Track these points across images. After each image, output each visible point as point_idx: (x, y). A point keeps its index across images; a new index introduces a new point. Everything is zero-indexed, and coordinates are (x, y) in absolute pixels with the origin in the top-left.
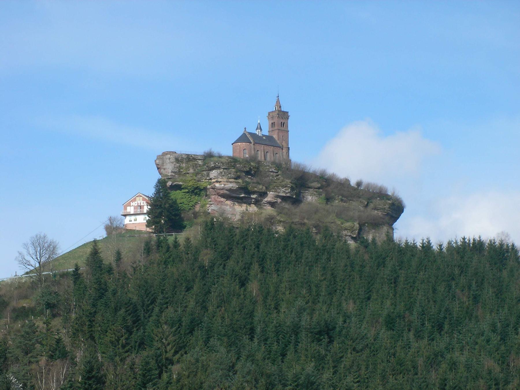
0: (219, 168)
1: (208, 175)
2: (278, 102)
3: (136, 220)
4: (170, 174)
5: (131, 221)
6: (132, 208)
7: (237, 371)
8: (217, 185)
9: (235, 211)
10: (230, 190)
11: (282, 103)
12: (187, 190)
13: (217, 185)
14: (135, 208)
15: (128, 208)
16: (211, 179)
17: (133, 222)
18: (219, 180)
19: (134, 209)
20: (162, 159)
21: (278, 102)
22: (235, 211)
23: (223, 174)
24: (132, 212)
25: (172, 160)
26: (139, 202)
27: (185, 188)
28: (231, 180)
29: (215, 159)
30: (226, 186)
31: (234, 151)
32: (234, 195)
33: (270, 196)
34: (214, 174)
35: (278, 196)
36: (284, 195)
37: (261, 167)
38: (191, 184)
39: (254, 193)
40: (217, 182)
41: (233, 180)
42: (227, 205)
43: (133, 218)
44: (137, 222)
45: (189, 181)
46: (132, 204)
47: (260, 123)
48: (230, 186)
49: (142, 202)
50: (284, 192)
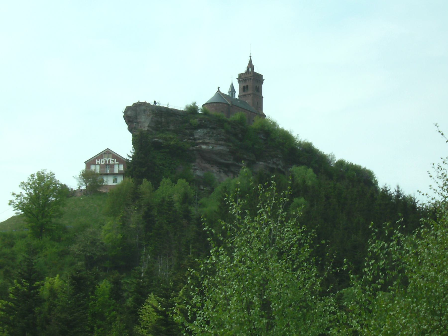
1: (192, 135)
2: (250, 62)
6: (98, 167)
8: (204, 147)
10: (219, 154)
13: (204, 147)
16: (195, 139)
18: (206, 141)
21: (250, 62)
26: (107, 160)
28: (220, 142)
34: (199, 133)
38: (172, 143)
40: (203, 143)
41: (222, 143)
48: (221, 148)
50: (274, 163)
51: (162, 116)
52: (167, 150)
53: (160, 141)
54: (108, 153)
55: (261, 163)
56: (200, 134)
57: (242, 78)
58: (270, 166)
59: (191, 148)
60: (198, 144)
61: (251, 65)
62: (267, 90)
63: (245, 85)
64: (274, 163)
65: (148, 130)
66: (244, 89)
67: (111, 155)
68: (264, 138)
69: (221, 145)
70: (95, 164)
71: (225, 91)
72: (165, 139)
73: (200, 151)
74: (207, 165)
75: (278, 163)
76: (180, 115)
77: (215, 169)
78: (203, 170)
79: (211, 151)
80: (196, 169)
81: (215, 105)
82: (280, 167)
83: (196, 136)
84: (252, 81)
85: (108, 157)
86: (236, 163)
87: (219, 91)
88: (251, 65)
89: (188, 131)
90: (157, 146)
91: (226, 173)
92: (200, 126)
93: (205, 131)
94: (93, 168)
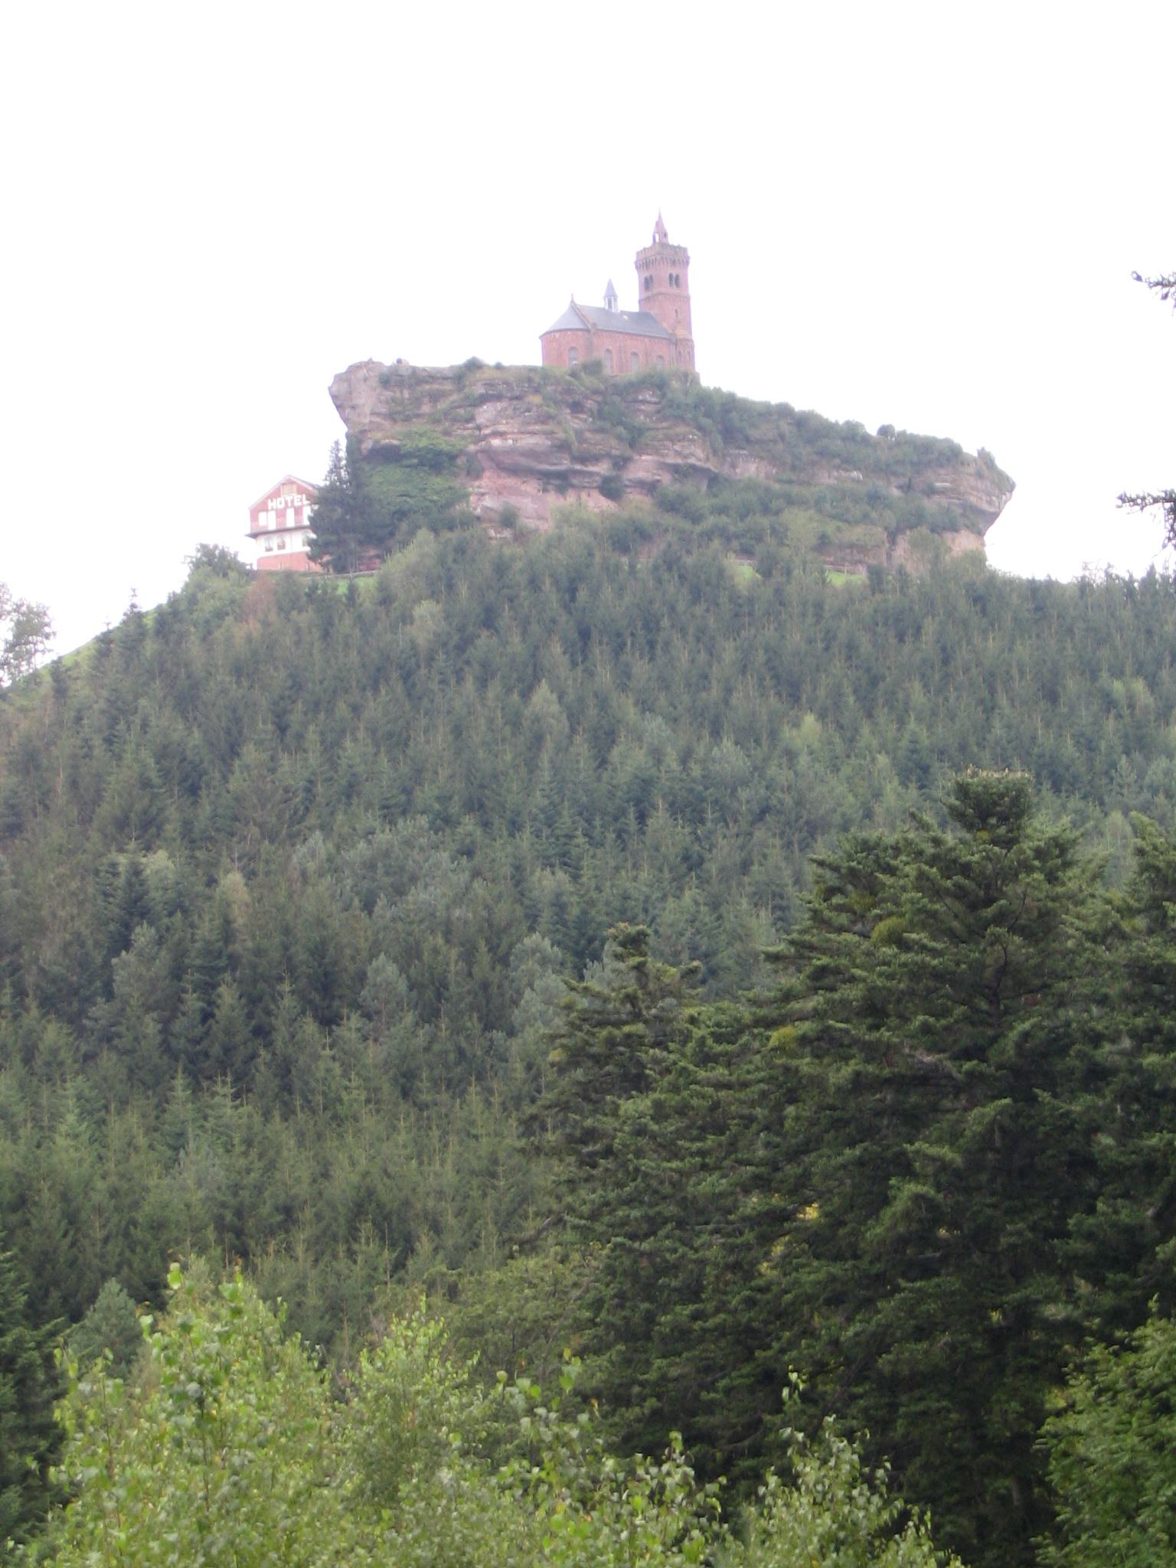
0: (499, 398)
1: (471, 419)
2: (659, 224)
3: (282, 546)
4: (367, 420)
5: (269, 550)
6: (272, 515)
8: (496, 442)
9: (539, 509)
10: (531, 453)
11: (668, 227)
12: (415, 461)
13: (496, 442)
14: (281, 514)
15: (262, 516)
16: (479, 428)
17: (276, 552)
18: (502, 428)
19: (278, 516)
20: (348, 381)
21: (659, 224)
22: (539, 509)
23: (510, 412)
24: (272, 527)
25: (374, 382)
26: (289, 499)
27: (410, 455)
29: (487, 375)
31: (546, 355)
32: (545, 467)
33: (643, 468)
34: (485, 413)
35: (664, 466)
36: (680, 461)
37: (619, 394)
38: (423, 443)
39: (596, 459)
40: (496, 434)
41: (537, 427)
42: (525, 494)
43: (275, 541)
44: (287, 551)
45: (422, 435)
46: (270, 504)
48: (528, 442)
49: (297, 497)
50: (678, 454)
51: (404, 387)
52: (415, 461)
53: (395, 442)
54: (289, 482)
55: (644, 457)
56: (487, 416)
57: (645, 262)
58: (670, 461)
59: (472, 448)
60: (485, 437)
61: (660, 230)
63: (647, 274)
64: (678, 454)
65: (371, 422)
67: (295, 487)
68: (654, 400)
70: (267, 511)
71: (594, 300)
72: (408, 435)
73: (489, 453)
74: (511, 481)
75: (686, 452)
76: (445, 378)
77: (531, 487)
78: (500, 493)
79: (511, 451)
80: (483, 494)
81: (557, 335)
82: (692, 461)
84: (663, 267)
86: (578, 467)
88: (660, 230)
89: (461, 411)
90: (388, 455)
91: (561, 490)
92: (483, 399)
93: (499, 406)
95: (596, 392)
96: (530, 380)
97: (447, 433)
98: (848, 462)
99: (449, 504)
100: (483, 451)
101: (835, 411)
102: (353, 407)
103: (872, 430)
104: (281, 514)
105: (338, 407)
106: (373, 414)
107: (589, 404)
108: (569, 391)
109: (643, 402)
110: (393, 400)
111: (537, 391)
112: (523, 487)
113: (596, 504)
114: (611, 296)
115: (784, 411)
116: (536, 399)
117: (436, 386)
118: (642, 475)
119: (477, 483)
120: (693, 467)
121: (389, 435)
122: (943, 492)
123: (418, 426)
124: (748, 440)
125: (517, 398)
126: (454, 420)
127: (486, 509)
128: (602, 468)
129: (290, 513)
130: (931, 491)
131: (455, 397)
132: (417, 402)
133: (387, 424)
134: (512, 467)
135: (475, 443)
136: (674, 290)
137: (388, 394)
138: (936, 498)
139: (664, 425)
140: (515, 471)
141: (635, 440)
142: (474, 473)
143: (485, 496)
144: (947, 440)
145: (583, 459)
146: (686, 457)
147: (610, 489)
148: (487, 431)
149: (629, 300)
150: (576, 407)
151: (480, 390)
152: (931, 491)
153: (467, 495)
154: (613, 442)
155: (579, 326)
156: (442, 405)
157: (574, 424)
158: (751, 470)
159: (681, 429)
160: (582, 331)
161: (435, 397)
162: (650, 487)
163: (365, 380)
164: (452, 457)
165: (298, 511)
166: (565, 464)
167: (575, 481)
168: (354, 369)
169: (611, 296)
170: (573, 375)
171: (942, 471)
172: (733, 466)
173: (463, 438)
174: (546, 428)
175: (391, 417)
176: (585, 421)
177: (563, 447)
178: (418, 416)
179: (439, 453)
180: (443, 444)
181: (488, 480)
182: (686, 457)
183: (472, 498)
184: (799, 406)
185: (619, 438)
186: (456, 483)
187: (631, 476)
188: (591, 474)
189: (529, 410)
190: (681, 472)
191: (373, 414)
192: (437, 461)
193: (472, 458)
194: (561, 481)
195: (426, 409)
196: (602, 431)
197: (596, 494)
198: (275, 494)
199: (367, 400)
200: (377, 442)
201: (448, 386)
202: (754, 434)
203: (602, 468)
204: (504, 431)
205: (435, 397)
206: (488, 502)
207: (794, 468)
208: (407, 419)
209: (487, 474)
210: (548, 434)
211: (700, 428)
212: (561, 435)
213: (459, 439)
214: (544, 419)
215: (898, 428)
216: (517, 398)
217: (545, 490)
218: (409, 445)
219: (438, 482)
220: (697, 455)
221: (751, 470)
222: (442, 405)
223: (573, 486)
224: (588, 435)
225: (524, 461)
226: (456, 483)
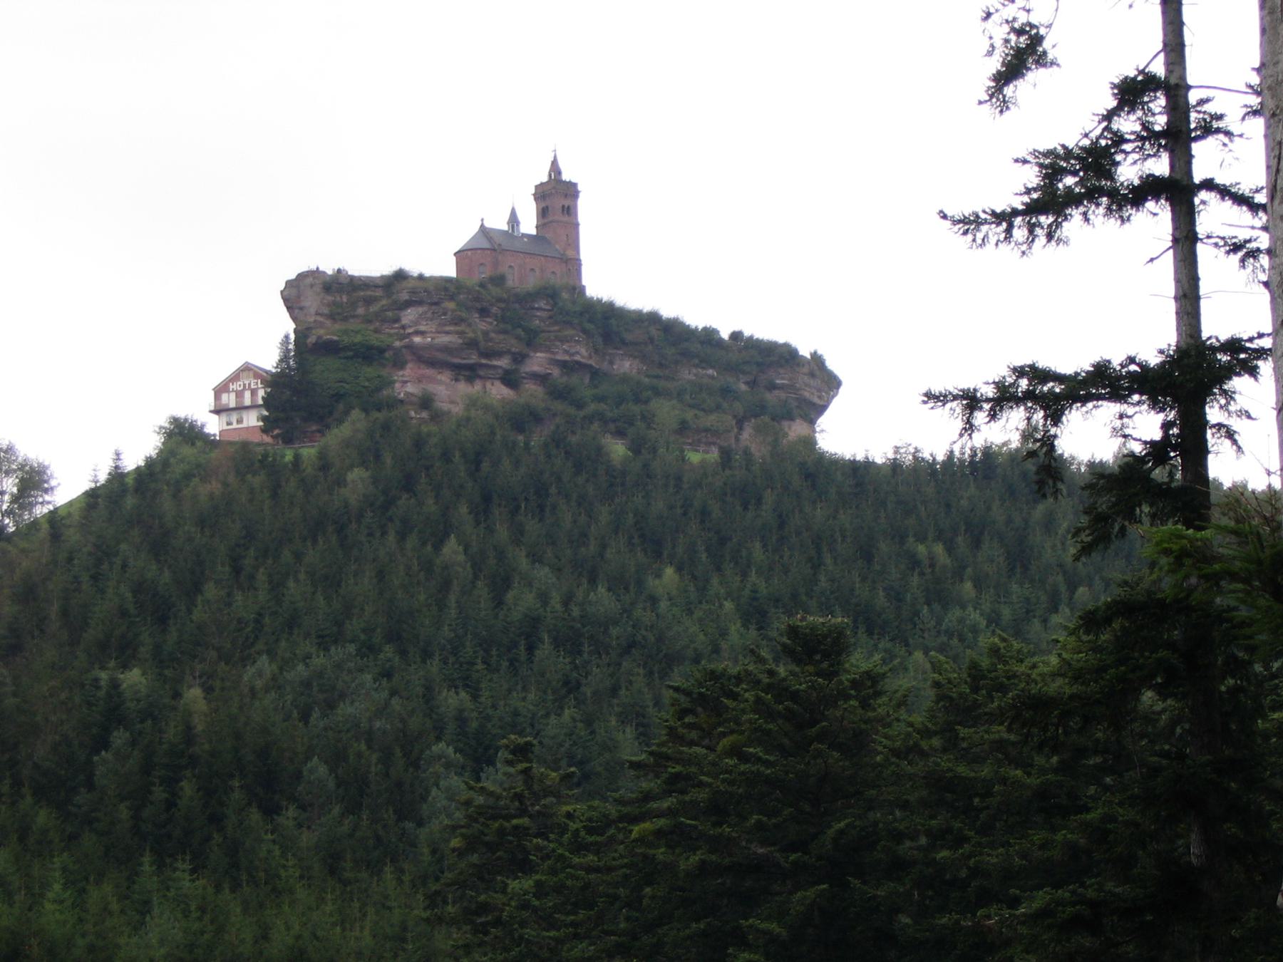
0: (420, 303)
1: (397, 320)
2: (555, 164)
3: (240, 421)
4: (312, 320)
5: (229, 424)
6: (233, 396)
7: (147, 903)
8: (417, 339)
9: (451, 394)
10: (446, 349)
11: (562, 165)
12: (351, 354)
13: (417, 339)
14: (239, 394)
16: (403, 327)
17: (235, 426)
18: (422, 328)
19: (237, 397)
20: (298, 287)
21: (555, 164)
22: (451, 394)
23: (429, 315)
24: (232, 405)
25: (318, 289)
27: (346, 348)
28: (447, 328)
29: (411, 284)
30: (436, 341)
33: (537, 362)
34: (409, 315)
36: (567, 358)
38: (358, 339)
39: (499, 354)
40: (418, 333)
41: (452, 328)
42: (440, 382)
44: (245, 425)
47: (512, 205)
48: (444, 339)
50: (566, 352)
52: (351, 354)
53: (335, 338)
54: (247, 369)
55: (538, 354)
56: (411, 317)
58: (559, 357)
59: (397, 344)
61: (555, 168)
62: (585, 210)
63: (544, 205)
64: (566, 352)
66: (543, 213)
67: (251, 374)
69: (447, 333)
70: (228, 392)
71: (499, 223)
72: (346, 332)
73: (411, 347)
74: (429, 372)
75: (573, 351)
76: (377, 286)
77: (445, 377)
79: (429, 347)
82: (577, 358)
83: (405, 321)
84: (557, 198)
85: (248, 377)
86: (484, 361)
87: (482, 225)
88: (555, 168)
89: (390, 314)
90: (328, 348)
91: (470, 380)
92: (408, 304)
93: (420, 310)
94: (224, 397)
95: (500, 300)
96: (446, 289)
97: (376, 331)
98: (705, 362)
99: (378, 389)
100: (407, 347)
101: (696, 319)
102: (301, 309)
103: (725, 335)
104: (239, 394)
105: (288, 308)
106: (317, 314)
107: (494, 310)
108: (477, 299)
109: (539, 309)
110: (334, 303)
111: (452, 298)
112: (439, 377)
113: (498, 391)
114: (514, 220)
115: (653, 318)
116: (451, 305)
117: (369, 293)
118: (536, 368)
119: (401, 373)
120: (578, 363)
121: (328, 332)
122: (782, 387)
123: (353, 325)
124: (624, 342)
125: (436, 304)
126: (384, 321)
127: (407, 394)
128: (504, 362)
129: (248, 395)
130: (772, 387)
131: (384, 302)
132: (353, 305)
133: (328, 323)
134: (431, 360)
135: (401, 340)
136: (566, 218)
137: (330, 298)
138: (776, 392)
139: (556, 328)
140: (432, 363)
141: (532, 340)
142: (399, 364)
143: (407, 383)
144: (786, 345)
145: (488, 355)
146: (572, 355)
147: (510, 380)
148: (410, 330)
149: (529, 225)
150: (484, 312)
151: (405, 296)
152: (772, 387)
153: (392, 383)
154: (513, 341)
155: (487, 245)
156: (374, 308)
157: (482, 325)
158: (626, 366)
159: (570, 332)
160: (487, 250)
161: (369, 301)
162: (542, 379)
163: (312, 286)
164: (381, 351)
165: (254, 393)
166: (474, 359)
167: (481, 373)
168: (302, 276)
169: (514, 220)
170: (482, 285)
171: (781, 371)
172: (611, 363)
173: (390, 335)
174: (458, 328)
175: (332, 317)
176: (491, 324)
177: (472, 344)
178: (354, 317)
179: (370, 348)
180: (374, 340)
181: (409, 371)
182: (572, 355)
183: (397, 385)
184: (667, 312)
185: (518, 338)
186: (384, 372)
187: (527, 369)
188: (495, 367)
189: (445, 314)
190: (569, 367)
191: (317, 314)
192: (370, 354)
193: (397, 352)
194: (469, 373)
195: (360, 311)
196: (505, 332)
197: (498, 383)
198: (235, 377)
199: (312, 302)
200: (319, 337)
201: (379, 293)
202: (628, 337)
203: (504, 362)
204: (424, 330)
205: (369, 301)
206: (410, 388)
207: (661, 365)
208: (345, 319)
209: (409, 365)
210: (461, 333)
211: (584, 331)
212: (471, 335)
213: (387, 336)
214: (457, 321)
215: (747, 333)
216: (436, 304)
217: (457, 380)
218: (346, 340)
219: (369, 371)
220: (582, 353)
221: (626, 366)
222: (374, 308)
223: (480, 377)
224: (493, 335)
225: (440, 356)
226: (384, 372)
